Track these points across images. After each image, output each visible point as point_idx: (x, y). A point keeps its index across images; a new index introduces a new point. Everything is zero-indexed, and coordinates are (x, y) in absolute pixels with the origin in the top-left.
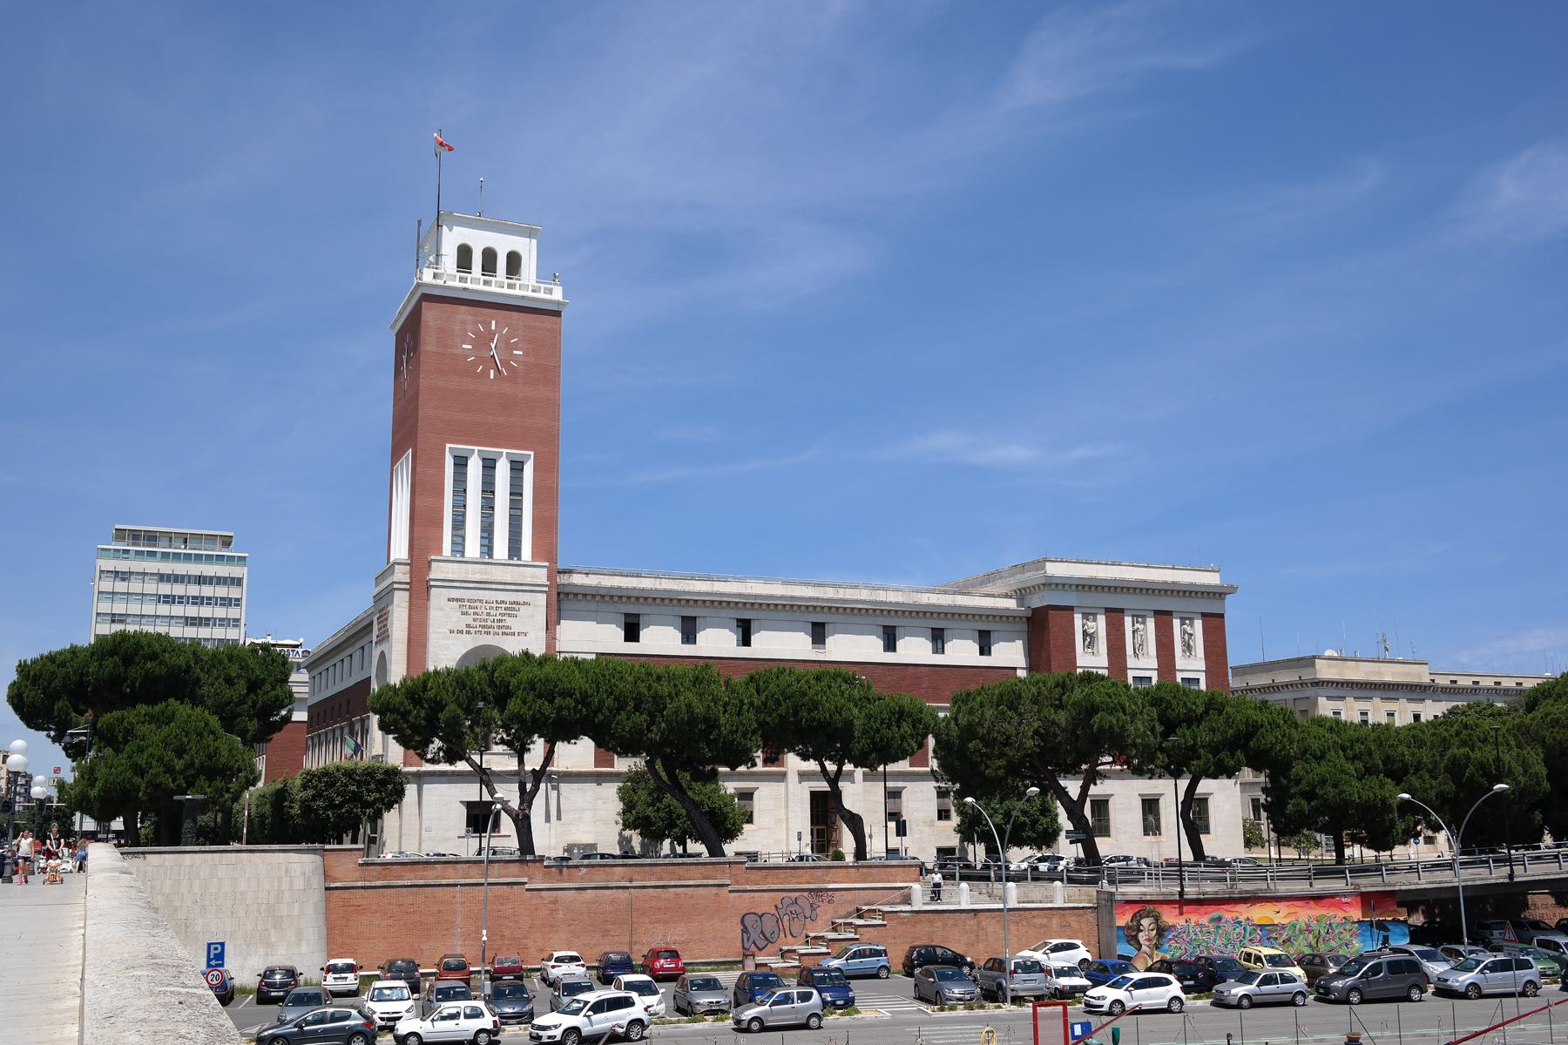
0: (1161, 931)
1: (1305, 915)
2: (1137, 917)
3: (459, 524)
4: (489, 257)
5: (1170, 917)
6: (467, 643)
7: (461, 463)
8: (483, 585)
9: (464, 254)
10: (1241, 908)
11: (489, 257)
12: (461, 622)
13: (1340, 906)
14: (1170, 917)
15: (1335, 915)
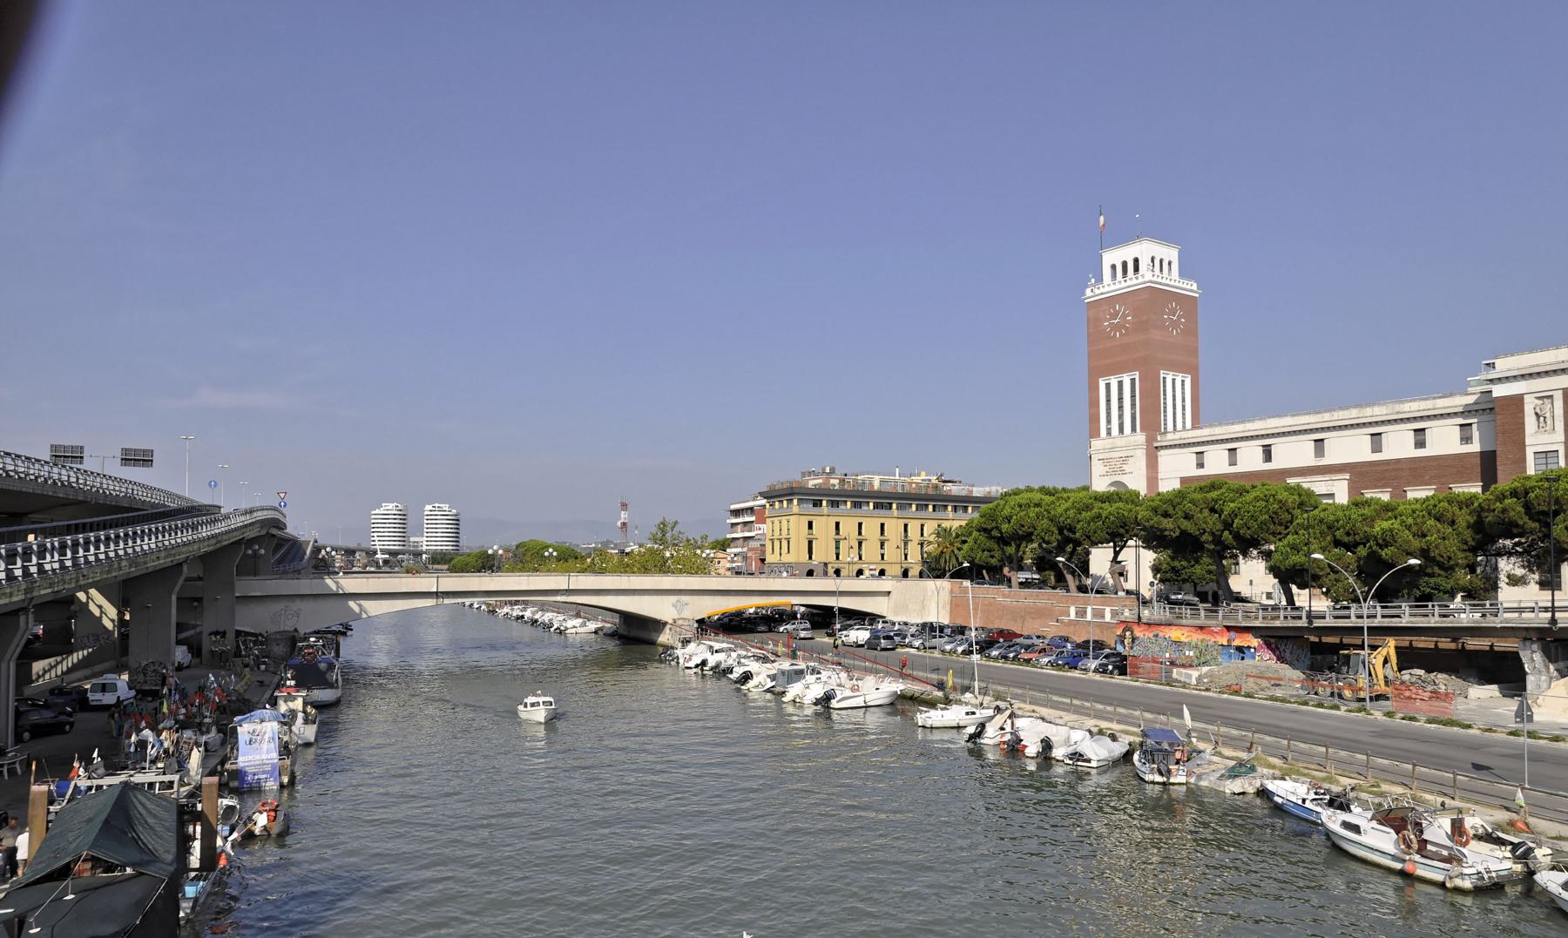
0: (1134, 639)
1: (1196, 637)
2: (1124, 631)
3: (1109, 421)
4: (1125, 264)
5: (1138, 632)
6: (1109, 480)
7: (1108, 386)
8: (1112, 449)
9: (1114, 267)
10: (1167, 629)
11: (1125, 264)
12: (1103, 470)
13: (1212, 633)
14: (1138, 632)
15: (1211, 639)
